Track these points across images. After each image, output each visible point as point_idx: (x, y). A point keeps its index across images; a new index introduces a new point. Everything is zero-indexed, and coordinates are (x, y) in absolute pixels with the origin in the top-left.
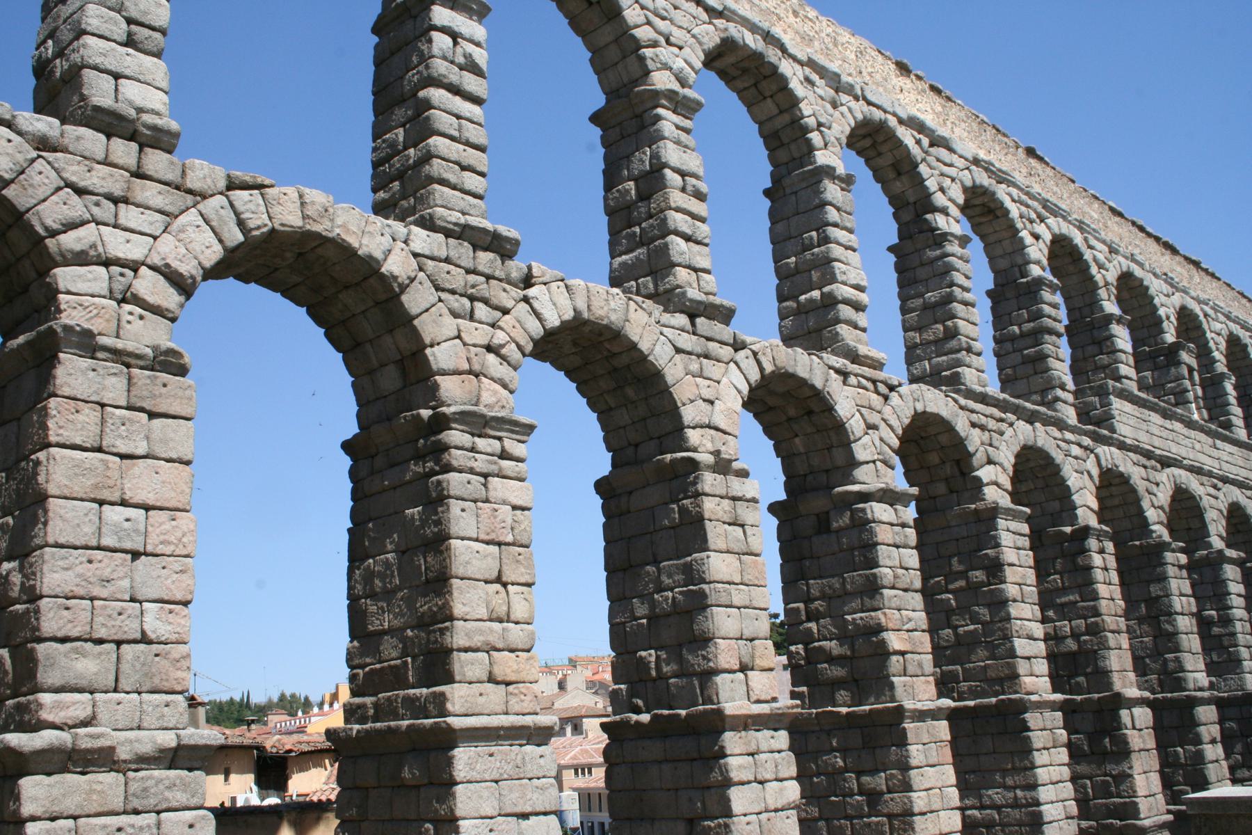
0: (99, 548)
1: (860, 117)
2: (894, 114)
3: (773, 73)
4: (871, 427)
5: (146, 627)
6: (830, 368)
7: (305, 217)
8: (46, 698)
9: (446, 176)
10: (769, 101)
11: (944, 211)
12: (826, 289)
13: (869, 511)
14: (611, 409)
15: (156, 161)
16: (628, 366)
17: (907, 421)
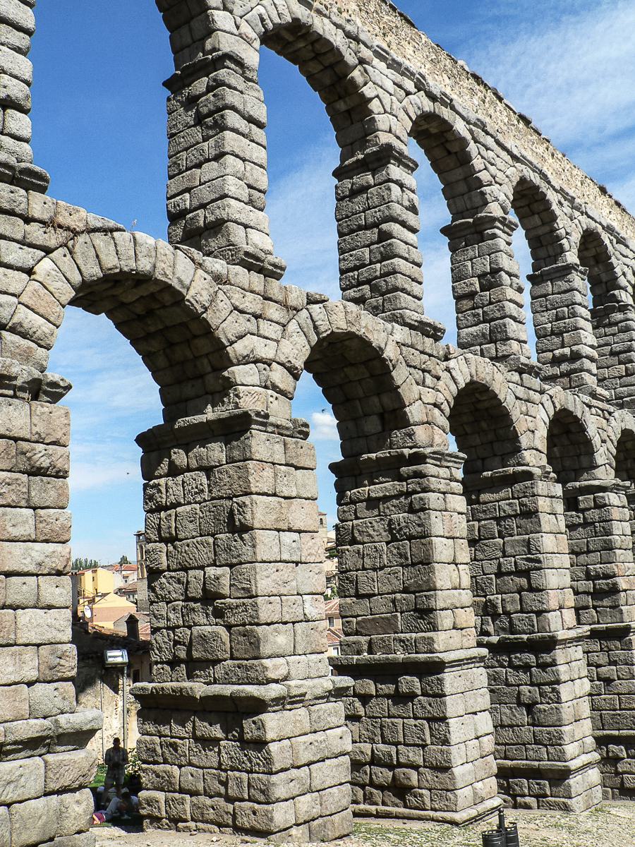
0: (280, 561)
1: (585, 227)
2: (600, 224)
3: (542, 199)
4: (604, 441)
5: (307, 612)
6: (584, 403)
7: (348, 322)
8: (266, 662)
9: (406, 286)
10: (536, 216)
11: (625, 289)
12: (574, 348)
13: (607, 499)
14: (467, 434)
15: (275, 287)
16: (487, 409)
17: (619, 436)
